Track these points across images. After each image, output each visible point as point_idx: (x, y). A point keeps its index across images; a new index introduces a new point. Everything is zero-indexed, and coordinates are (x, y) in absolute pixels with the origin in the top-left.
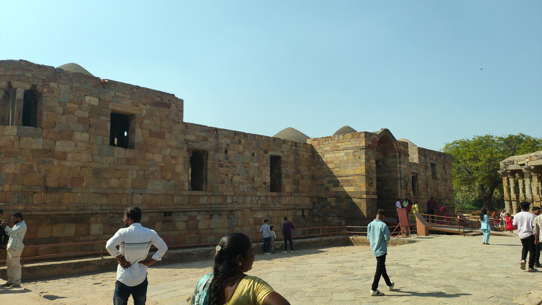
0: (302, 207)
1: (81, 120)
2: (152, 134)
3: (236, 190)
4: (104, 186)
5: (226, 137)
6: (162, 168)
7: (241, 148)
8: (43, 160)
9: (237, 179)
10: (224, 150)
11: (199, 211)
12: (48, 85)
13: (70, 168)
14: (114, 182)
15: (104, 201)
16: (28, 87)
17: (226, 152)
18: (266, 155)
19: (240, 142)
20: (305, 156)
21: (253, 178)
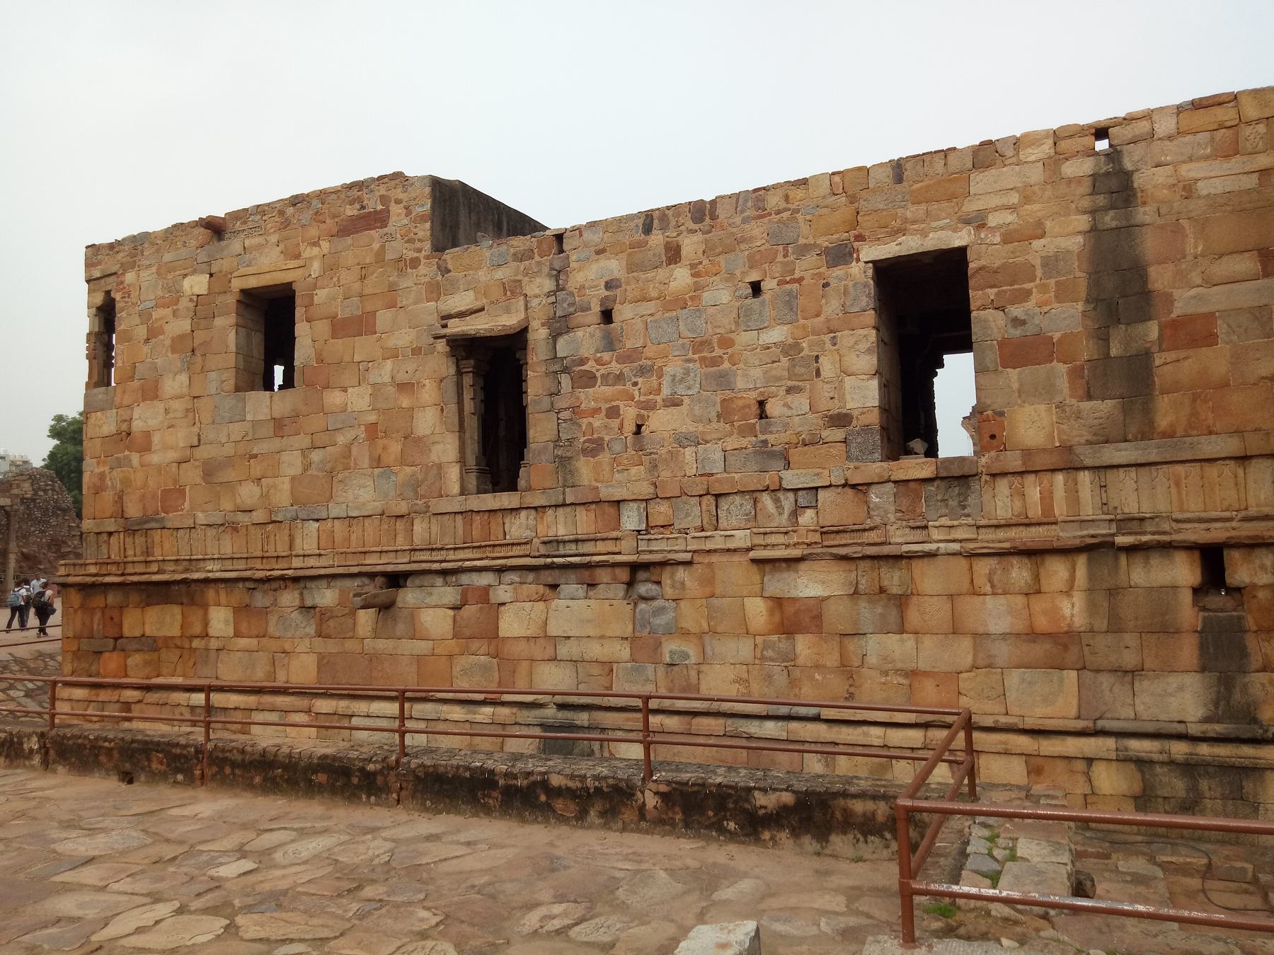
2: (341, 328)
4: (227, 505)
5: (599, 252)
6: (372, 430)
7: (681, 277)
9: (662, 422)
10: (596, 308)
11: (501, 570)
13: (159, 468)
14: (248, 493)
15: (228, 546)
17: (607, 316)
18: (838, 272)
19: (673, 254)
20: (1203, 188)
21: (761, 404)
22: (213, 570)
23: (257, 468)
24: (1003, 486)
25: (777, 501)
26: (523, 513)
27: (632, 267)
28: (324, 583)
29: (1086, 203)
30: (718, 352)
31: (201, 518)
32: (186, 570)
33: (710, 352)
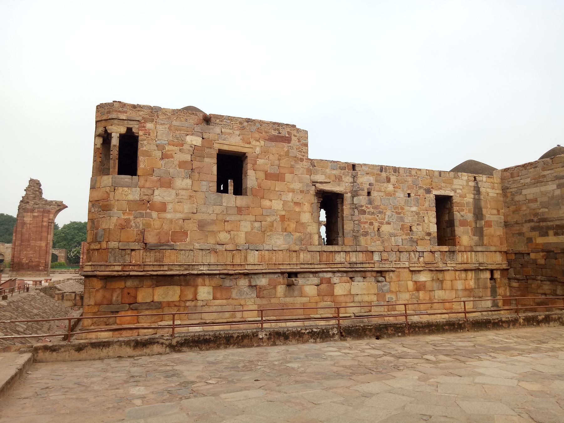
0: (490, 267)
1: (182, 164)
2: (268, 176)
3: (386, 244)
4: (212, 241)
5: (367, 174)
6: (283, 218)
7: (390, 187)
8: (140, 213)
9: (385, 229)
10: (366, 191)
11: (334, 272)
12: (144, 127)
13: (171, 221)
14: (223, 237)
15: (212, 259)
16: (123, 130)
17: (369, 194)
18: (428, 195)
19: (388, 180)
20: (490, 194)
21: (410, 227)
22: (204, 269)
23: (228, 227)
24: (460, 253)
25: (415, 254)
26: (342, 253)
27: (377, 181)
28: (261, 276)
29: (473, 192)
30: (400, 211)
31: (197, 246)
32: (186, 269)
33: (399, 211)
